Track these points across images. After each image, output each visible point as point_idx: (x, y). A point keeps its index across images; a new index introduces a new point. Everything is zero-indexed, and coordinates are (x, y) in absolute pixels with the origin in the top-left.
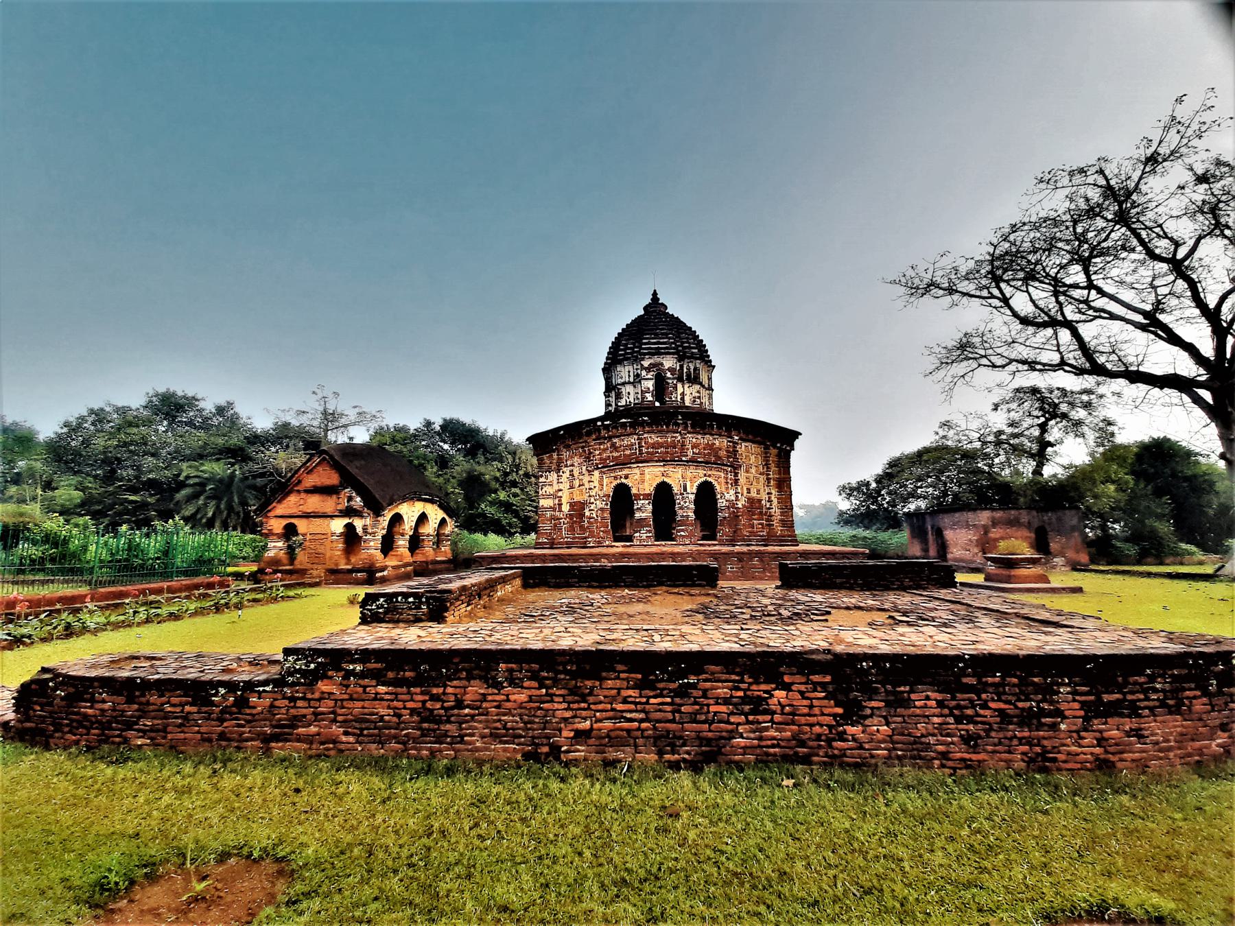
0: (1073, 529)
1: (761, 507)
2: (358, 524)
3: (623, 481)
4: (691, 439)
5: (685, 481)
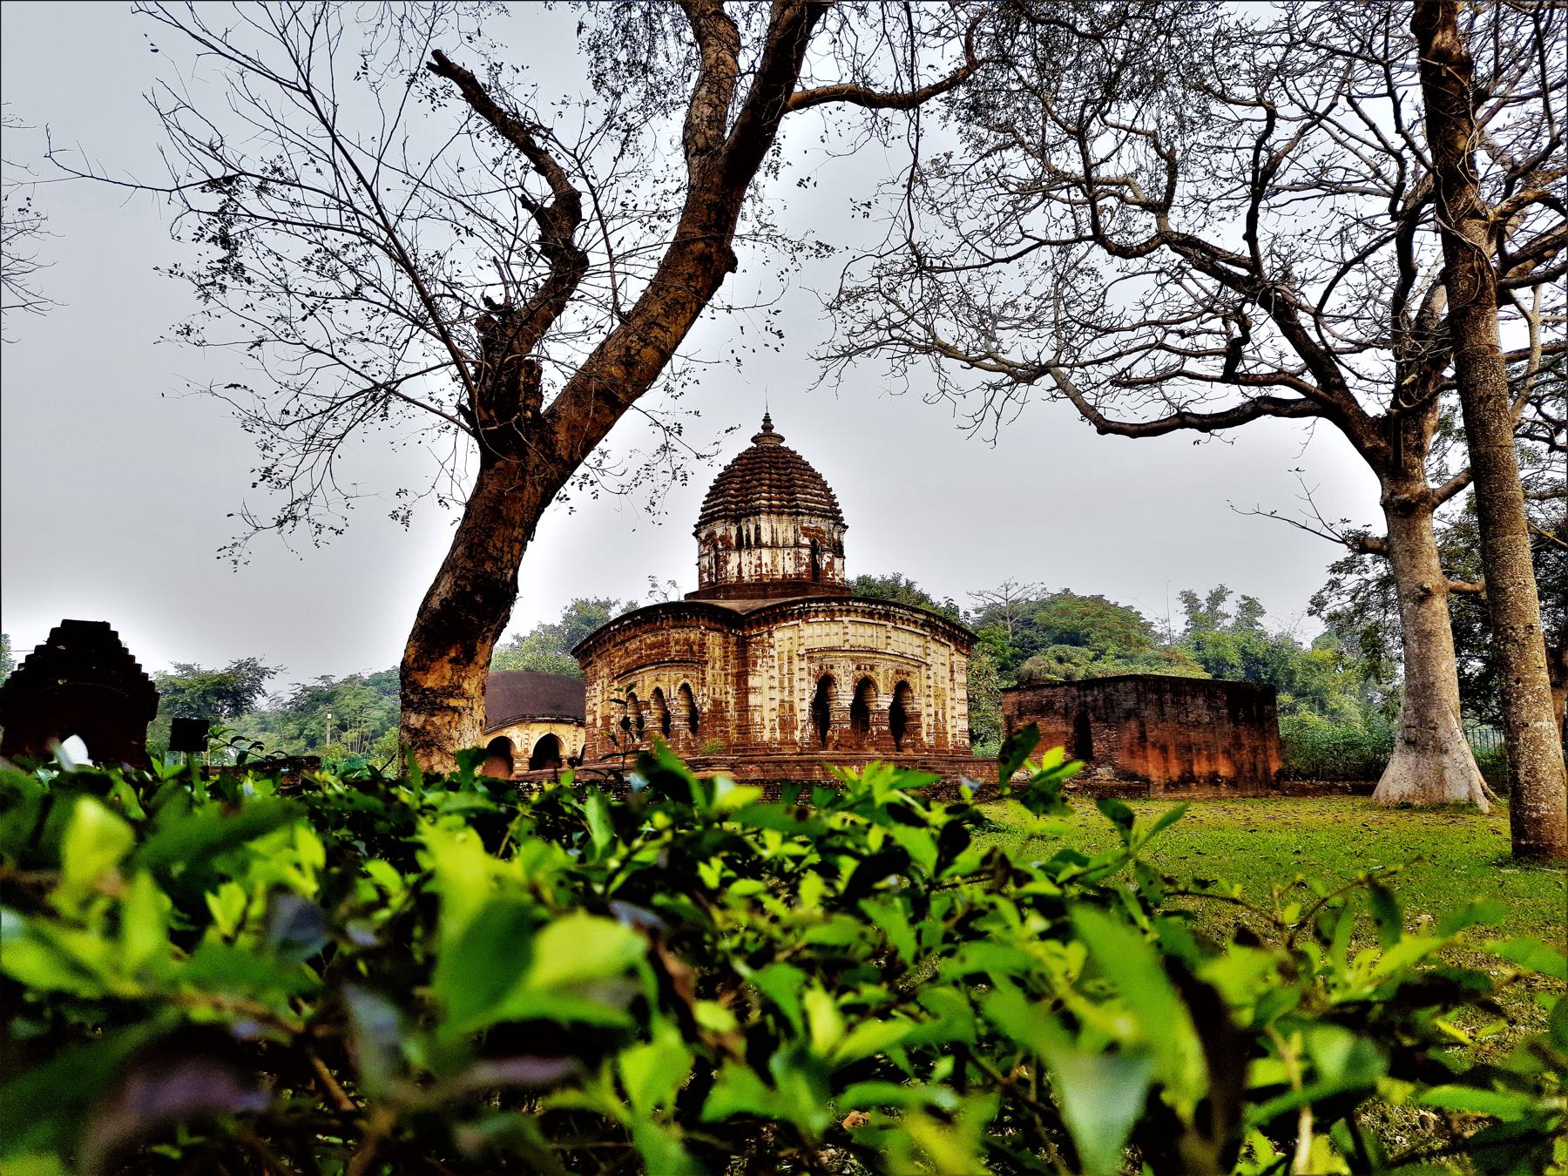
0: (1130, 714)
4: (675, 634)
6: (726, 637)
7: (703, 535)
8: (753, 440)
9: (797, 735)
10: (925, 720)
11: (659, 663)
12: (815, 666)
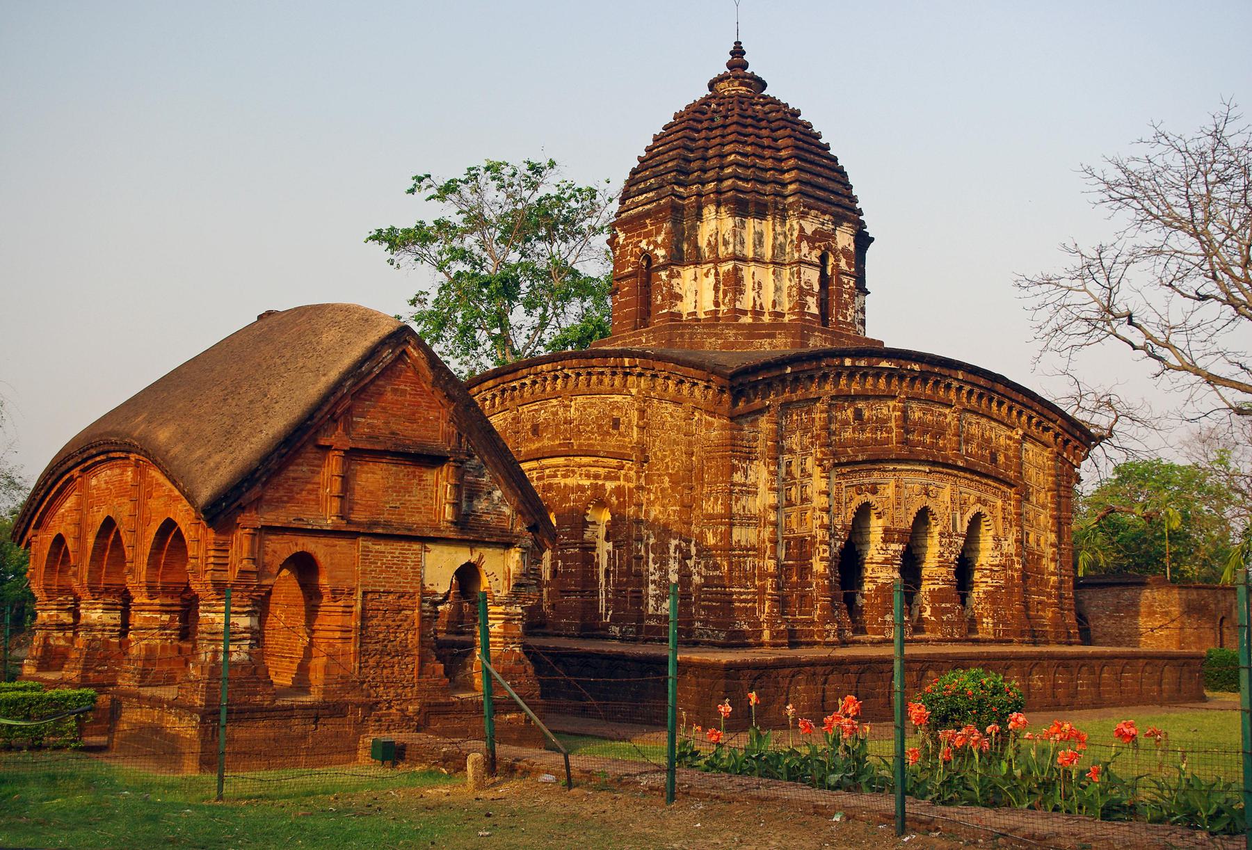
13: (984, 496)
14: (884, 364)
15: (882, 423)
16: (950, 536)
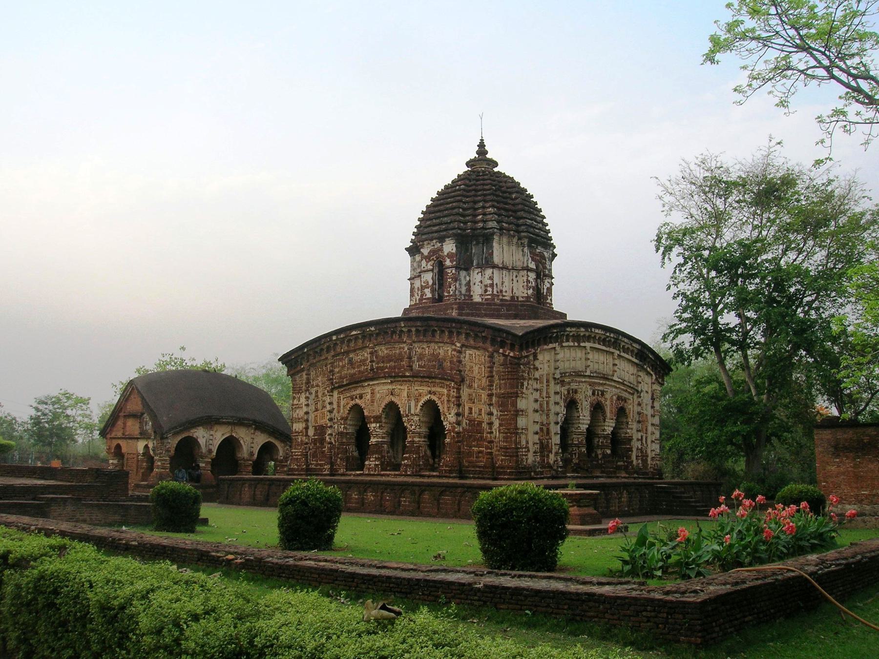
1: (481, 432)
2: (151, 446)
3: (358, 401)
4: (418, 348)
5: (410, 399)
6: (491, 356)
7: (425, 251)
8: (468, 164)
9: (552, 458)
10: (635, 444)
11: (396, 376)
12: (564, 390)
13: (433, 389)
14: (354, 333)
15: (363, 362)
16: (407, 416)
